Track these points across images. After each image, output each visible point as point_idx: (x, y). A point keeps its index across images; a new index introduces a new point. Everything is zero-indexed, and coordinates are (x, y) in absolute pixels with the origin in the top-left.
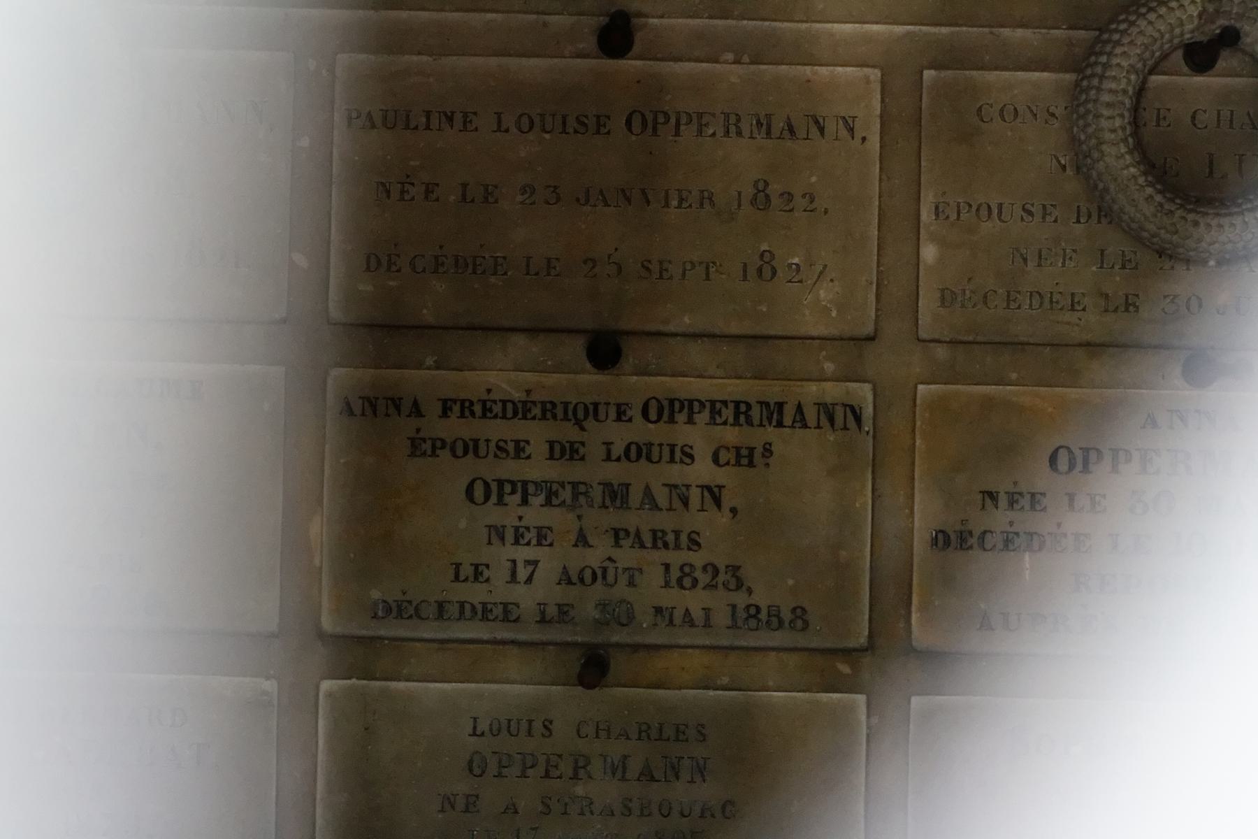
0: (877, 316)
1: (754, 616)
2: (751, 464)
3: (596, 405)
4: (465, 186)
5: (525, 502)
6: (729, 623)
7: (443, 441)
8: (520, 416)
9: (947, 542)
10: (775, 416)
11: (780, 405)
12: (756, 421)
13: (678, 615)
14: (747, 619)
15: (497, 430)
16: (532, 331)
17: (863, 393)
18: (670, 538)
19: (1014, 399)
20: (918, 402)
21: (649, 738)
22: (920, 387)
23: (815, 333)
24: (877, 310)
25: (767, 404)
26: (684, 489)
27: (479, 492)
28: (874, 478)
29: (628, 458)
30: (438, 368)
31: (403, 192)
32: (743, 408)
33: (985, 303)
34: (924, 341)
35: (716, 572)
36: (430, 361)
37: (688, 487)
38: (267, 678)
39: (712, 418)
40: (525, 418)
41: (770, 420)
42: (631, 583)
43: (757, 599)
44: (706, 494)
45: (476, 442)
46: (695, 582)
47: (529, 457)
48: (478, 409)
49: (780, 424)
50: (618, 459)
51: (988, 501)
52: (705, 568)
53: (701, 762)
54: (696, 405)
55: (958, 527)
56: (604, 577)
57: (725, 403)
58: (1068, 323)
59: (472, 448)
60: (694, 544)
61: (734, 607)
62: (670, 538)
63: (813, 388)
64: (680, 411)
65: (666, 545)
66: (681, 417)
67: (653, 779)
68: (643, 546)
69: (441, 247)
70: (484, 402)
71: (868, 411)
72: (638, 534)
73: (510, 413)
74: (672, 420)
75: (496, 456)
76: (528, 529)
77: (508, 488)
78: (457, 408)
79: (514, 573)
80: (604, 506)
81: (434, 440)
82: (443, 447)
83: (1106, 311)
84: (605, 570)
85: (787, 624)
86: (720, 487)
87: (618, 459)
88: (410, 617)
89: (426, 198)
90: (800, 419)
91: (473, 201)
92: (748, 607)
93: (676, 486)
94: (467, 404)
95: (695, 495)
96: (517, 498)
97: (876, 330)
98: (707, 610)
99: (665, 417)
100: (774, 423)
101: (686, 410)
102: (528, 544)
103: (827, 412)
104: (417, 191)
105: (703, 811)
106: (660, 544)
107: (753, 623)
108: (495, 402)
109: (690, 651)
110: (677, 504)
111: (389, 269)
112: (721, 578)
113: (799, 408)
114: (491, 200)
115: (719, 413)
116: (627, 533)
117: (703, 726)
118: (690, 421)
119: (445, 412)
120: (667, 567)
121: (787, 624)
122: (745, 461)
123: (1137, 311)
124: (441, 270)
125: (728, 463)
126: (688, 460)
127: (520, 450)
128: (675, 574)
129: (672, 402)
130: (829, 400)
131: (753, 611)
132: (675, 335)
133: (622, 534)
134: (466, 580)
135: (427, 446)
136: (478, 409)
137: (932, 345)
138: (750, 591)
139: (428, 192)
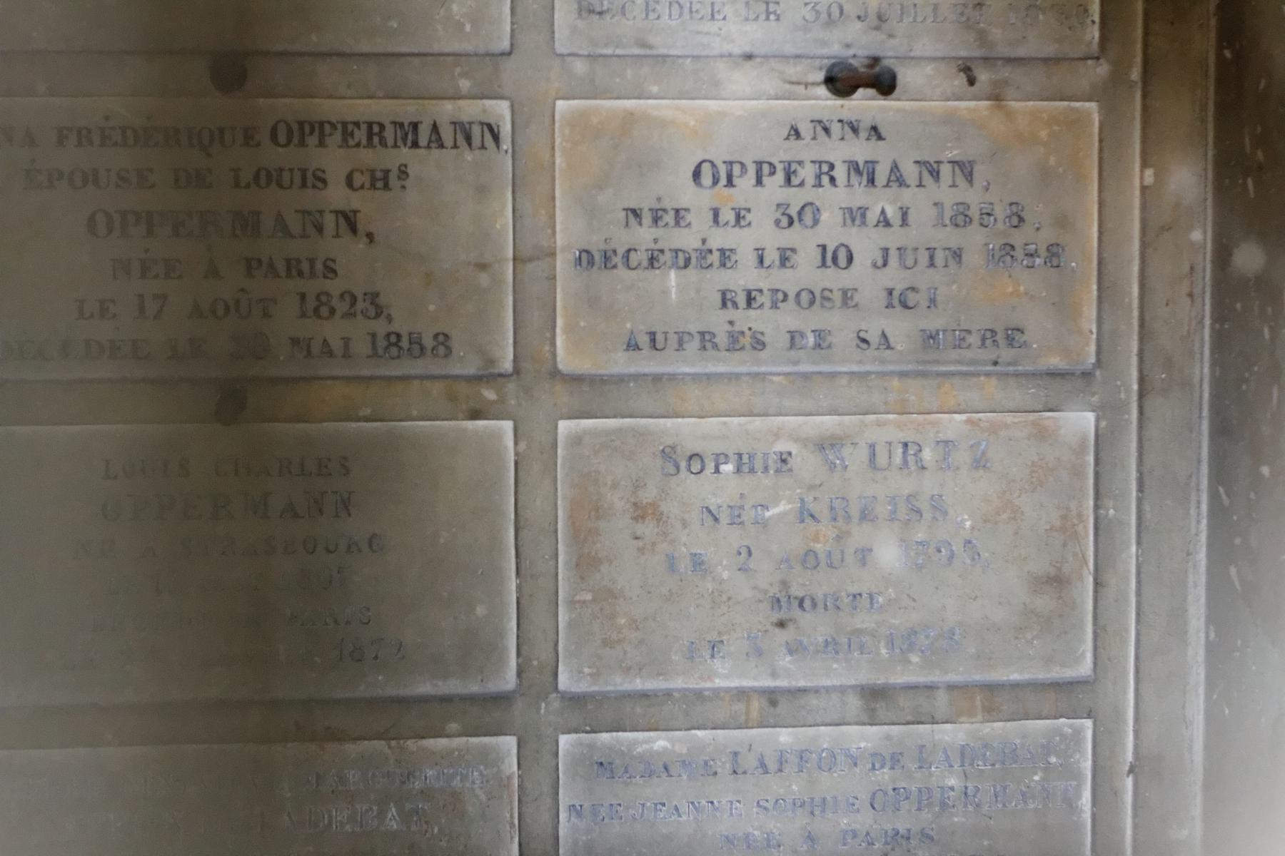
0: (512, 30)
1: (396, 344)
2: (386, 186)
3: (222, 131)
6: (370, 352)
9: (591, 263)
10: (410, 137)
11: (415, 126)
12: (390, 141)
13: (316, 348)
14: (387, 348)
17: (500, 110)
18: (305, 266)
19: (656, 113)
20: (557, 117)
21: (290, 472)
22: (560, 103)
23: (447, 50)
24: (512, 24)
25: (402, 125)
26: (317, 215)
28: (514, 199)
29: (258, 184)
32: (376, 129)
33: (624, 14)
34: (562, 55)
35: (354, 300)
37: (321, 212)
39: (345, 140)
41: (404, 139)
42: (266, 315)
43: (396, 327)
44: (342, 220)
46: (332, 311)
49: (415, 145)
50: (248, 186)
51: (631, 216)
52: (342, 296)
53: (346, 496)
54: (327, 128)
55: (603, 247)
56: (237, 310)
57: (357, 124)
58: (707, 33)
60: (331, 272)
61: (374, 336)
62: (305, 266)
63: (448, 106)
64: (311, 133)
65: (300, 274)
66: (312, 140)
67: (296, 516)
68: (277, 276)
71: (506, 130)
72: (271, 265)
74: (302, 143)
75: (118, 186)
79: (142, 310)
80: (236, 236)
83: (747, 19)
84: (237, 302)
85: (429, 352)
86: (355, 212)
87: (248, 186)
90: (436, 139)
92: (388, 335)
93: (309, 213)
95: (329, 221)
97: (512, 45)
98: (346, 341)
99: (296, 140)
100: (409, 143)
101: (316, 133)
102: (156, 277)
103: (464, 132)
105: (349, 547)
106: (294, 272)
107: (394, 351)
109: (329, 382)
110: (311, 230)
112: (360, 305)
113: (435, 127)
115: (352, 134)
116: (260, 261)
117: (345, 458)
118: (321, 144)
120: (303, 297)
121: (429, 352)
122: (380, 184)
123: (778, 19)
125: (362, 187)
126: (320, 184)
128: (311, 303)
129: (301, 124)
130: (465, 119)
131: (393, 339)
132: (302, 54)
133: (254, 264)
137: (570, 59)
138: (390, 319)
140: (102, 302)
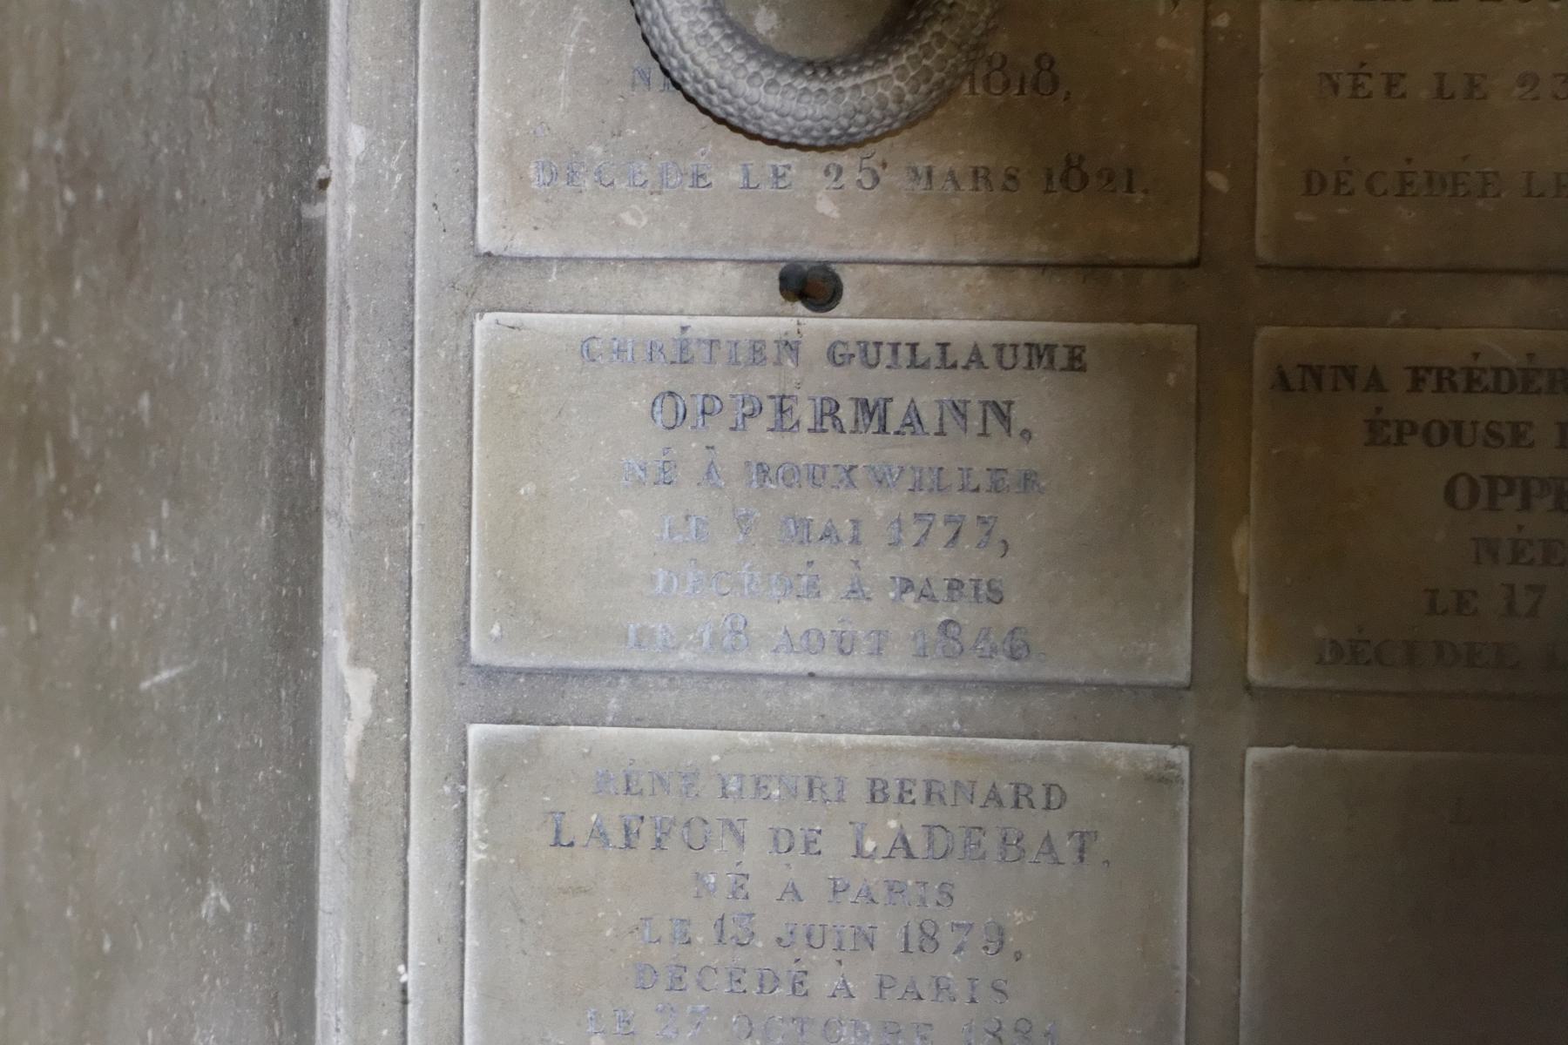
4: (1441, 76)
5: (1526, 505)
7: (1412, 424)
8: (1519, 389)
15: (1484, 408)
16: (1539, 273)
27: (1462, 495)
30: (1407, 326)
31: (1355, 87)
36: (1396, 316)
38: (1174, 745)
40: (1525, 391)
45: (1459, 425)
47: (1531, 445)
48: (1460, 379)
59: (1452, 433)
69: (1409, 160)
70: (1469, 371)
73: (1505, 386)
76: (1530, 542)
77: (1502, 488)
78: (1432, 380)
79: (1511, 608)
81: (1400, 424)
82: (1414, 431)
88: (1368, 663)
89: (1389, 93)
91: (1452, 97)
94: (1445, 374)
96: (1515, 500)
102: (1531, 562)
104: (1375, 85)
108: (1483, 370)
111: (1337, 192)
114: (1476, 94)
119: (1417, 383)
124: (1409, 191)
127: (1518, 435)
134: (1445, 612)
135: (1391, 431)
136: (1460, 379)
139: (1390, 86)
140: (1460, 595)
